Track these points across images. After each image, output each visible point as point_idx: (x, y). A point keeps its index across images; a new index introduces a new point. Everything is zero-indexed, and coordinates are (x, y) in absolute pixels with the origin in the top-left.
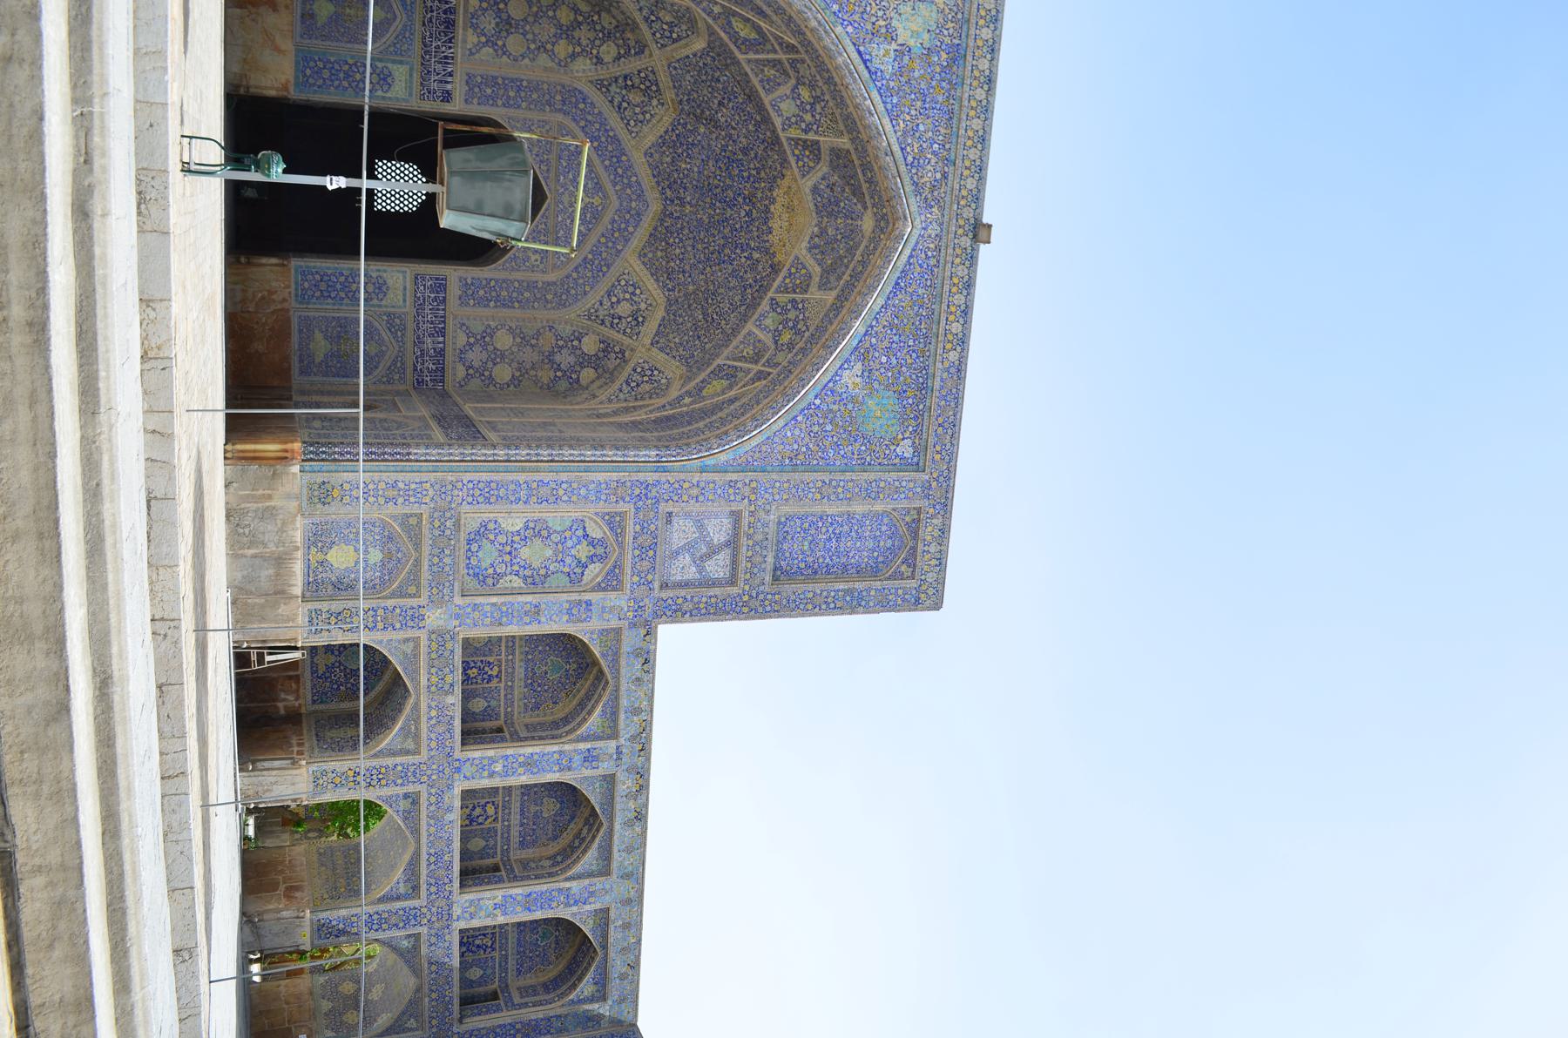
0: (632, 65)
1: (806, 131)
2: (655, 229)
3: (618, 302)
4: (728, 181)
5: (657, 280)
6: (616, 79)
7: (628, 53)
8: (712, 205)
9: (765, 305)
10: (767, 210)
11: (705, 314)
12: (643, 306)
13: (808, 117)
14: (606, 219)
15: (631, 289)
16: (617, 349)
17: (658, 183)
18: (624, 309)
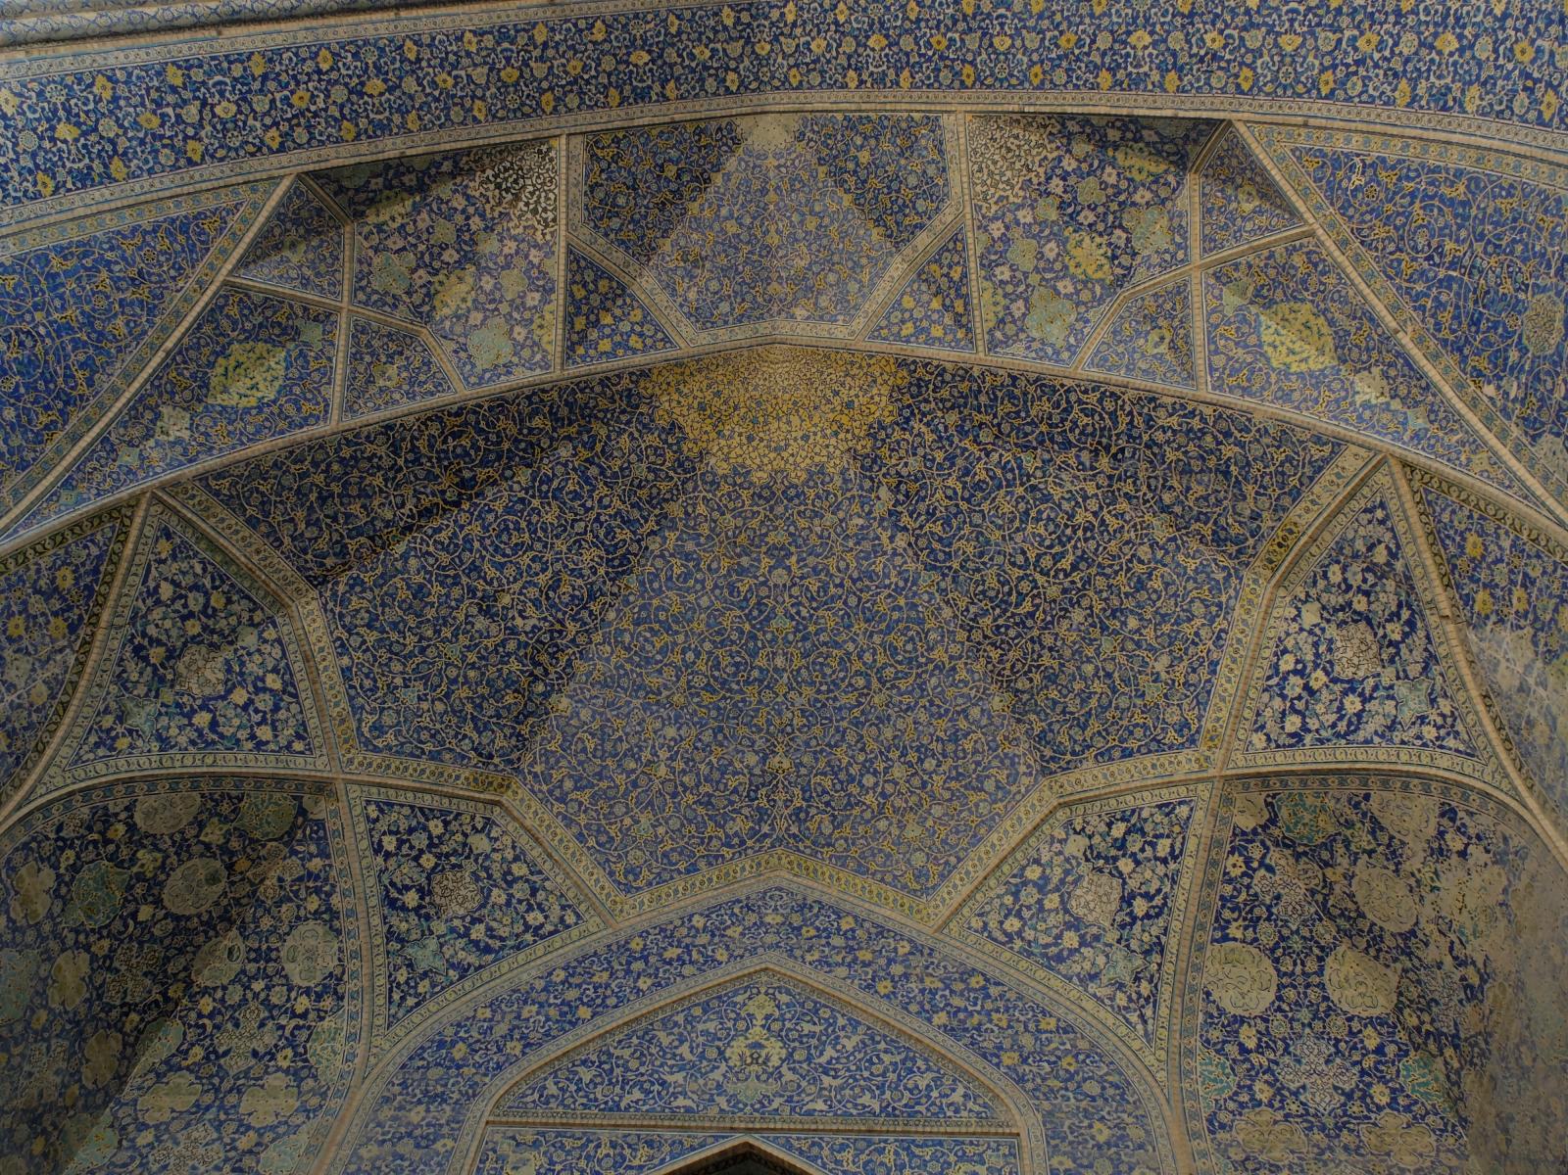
0: (356, 870)
1: (547, 291)
2: (841, 861)
3: (1076, 924)
4: (699, 627)
5: (990, 823)
6: (391, 935)
7: (318, 884)
8: (766, 682)
9: (1016, 358)
10: (766, 495)
11: (1073, 597)
12: (1076, 846)
13: (512, 283)
14: (818, 979)
15: (1029, 896)
16: (1235, 865)
17: (714, 859)
18: (1096, 900)
